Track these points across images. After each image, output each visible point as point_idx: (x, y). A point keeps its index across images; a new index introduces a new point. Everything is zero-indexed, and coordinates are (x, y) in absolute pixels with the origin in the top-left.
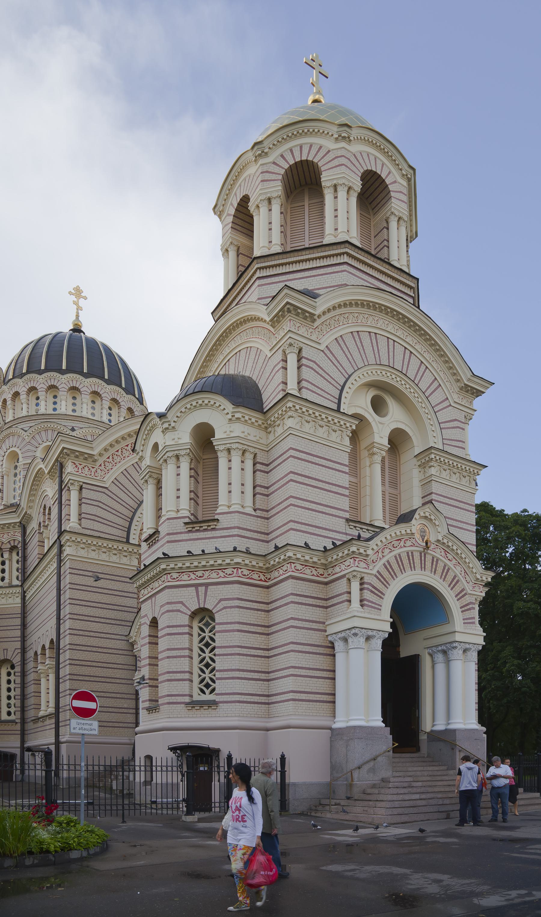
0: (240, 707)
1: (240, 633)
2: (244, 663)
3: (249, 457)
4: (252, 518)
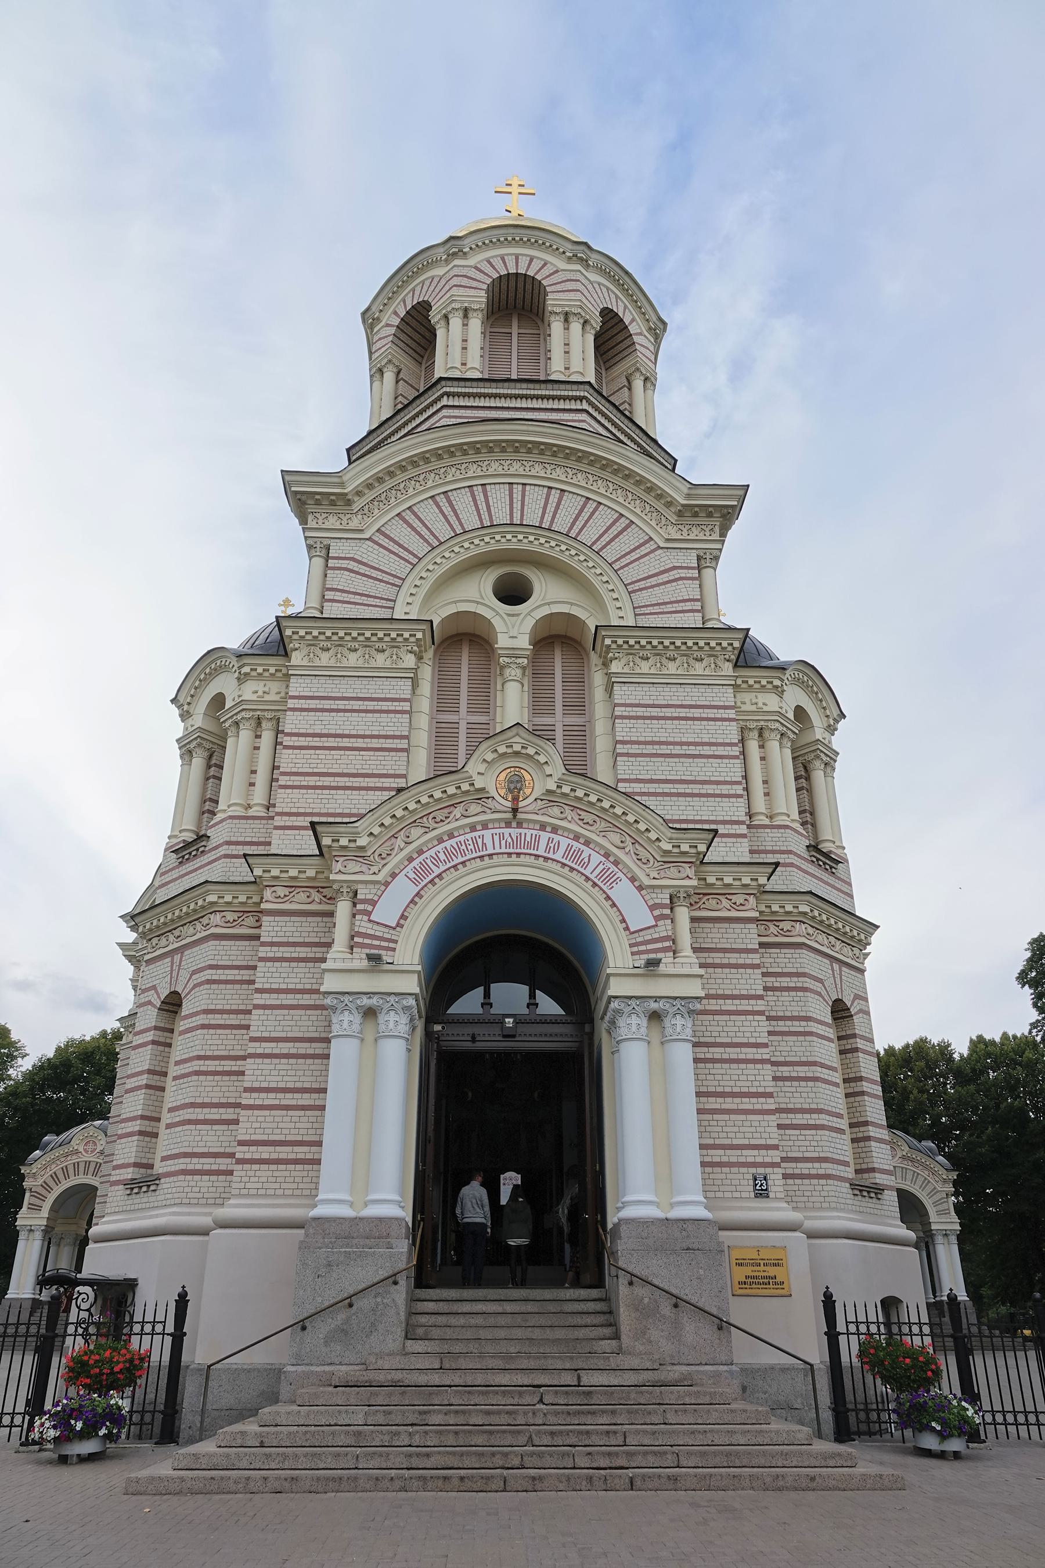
0: (186, 1184)
1: (205, 1031)
2: (207, 1089)
4: (258, 822)
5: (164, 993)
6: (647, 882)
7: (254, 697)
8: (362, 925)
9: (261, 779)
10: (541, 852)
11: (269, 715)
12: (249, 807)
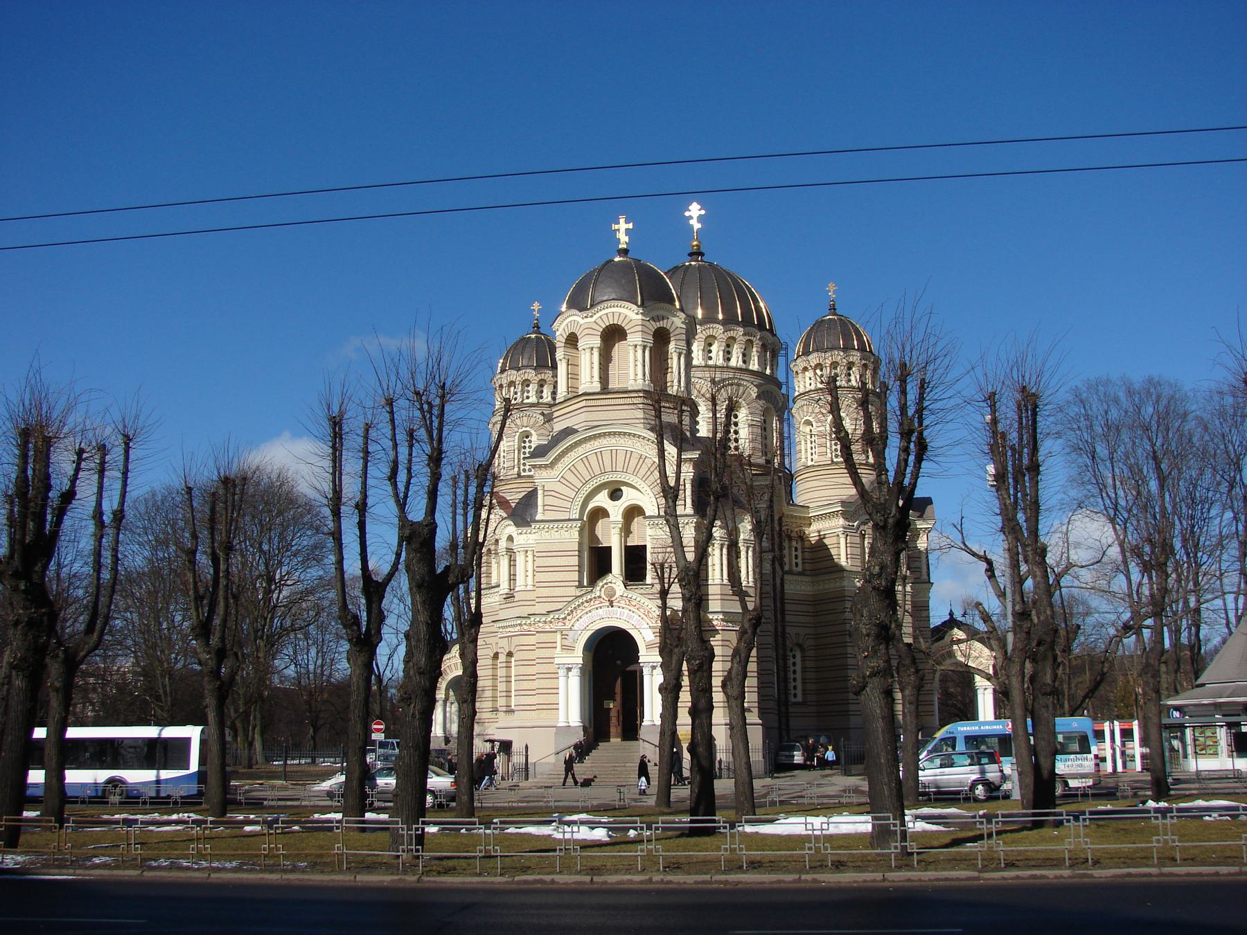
3: (530, 554)
5: (507, 651)
6: (651, 625)
7: (524, 542)
8: (565, 642)
9: (530, 574)
10: (618, 616)
11: (530, 549)
12: (526, 586)
